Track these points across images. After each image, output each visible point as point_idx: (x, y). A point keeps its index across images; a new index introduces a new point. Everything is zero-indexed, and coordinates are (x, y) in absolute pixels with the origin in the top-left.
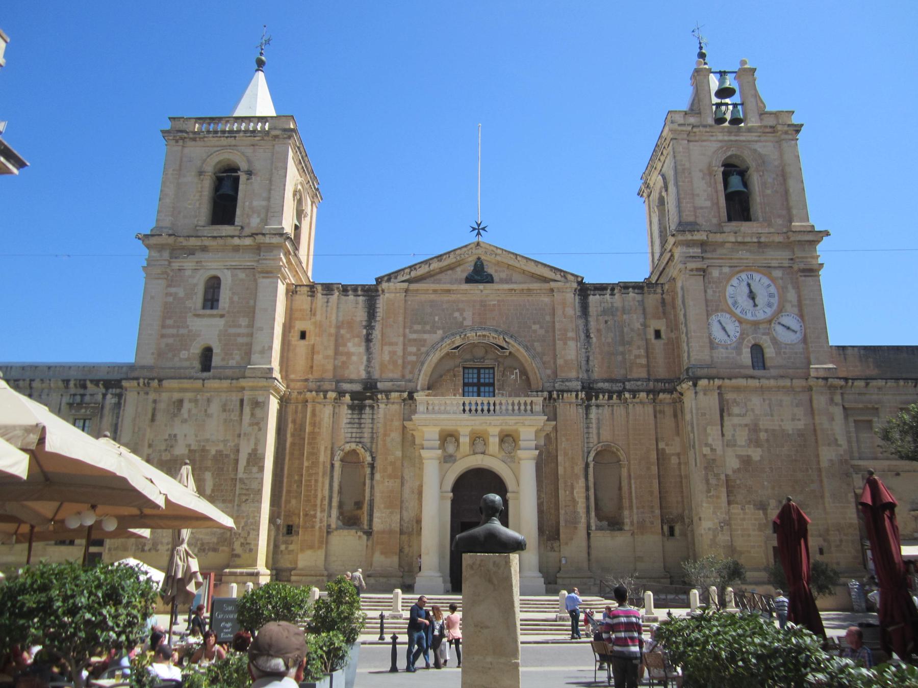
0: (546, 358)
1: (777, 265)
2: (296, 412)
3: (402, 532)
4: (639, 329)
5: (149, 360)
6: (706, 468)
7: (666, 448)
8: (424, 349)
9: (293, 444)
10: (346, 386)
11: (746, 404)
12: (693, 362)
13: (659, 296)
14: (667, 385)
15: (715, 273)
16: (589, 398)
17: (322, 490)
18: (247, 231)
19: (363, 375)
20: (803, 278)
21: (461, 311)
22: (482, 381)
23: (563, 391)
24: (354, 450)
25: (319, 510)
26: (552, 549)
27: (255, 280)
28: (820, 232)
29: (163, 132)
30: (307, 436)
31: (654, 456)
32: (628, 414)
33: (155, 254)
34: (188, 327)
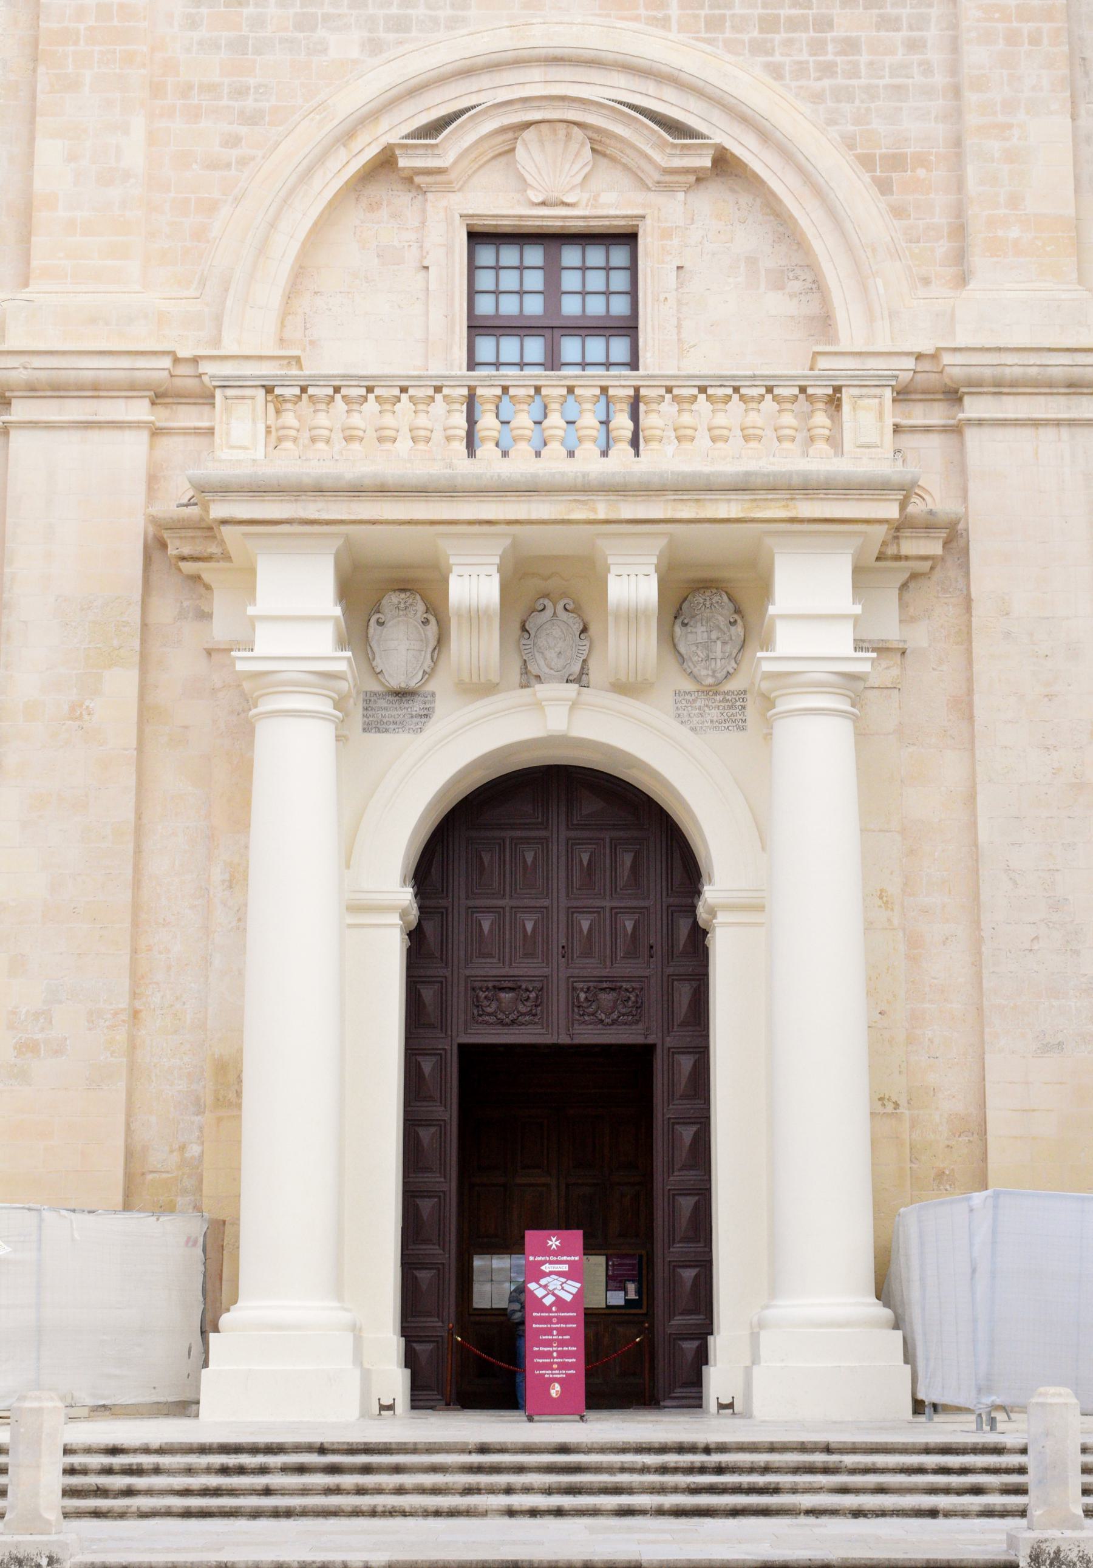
22: (571, 306)
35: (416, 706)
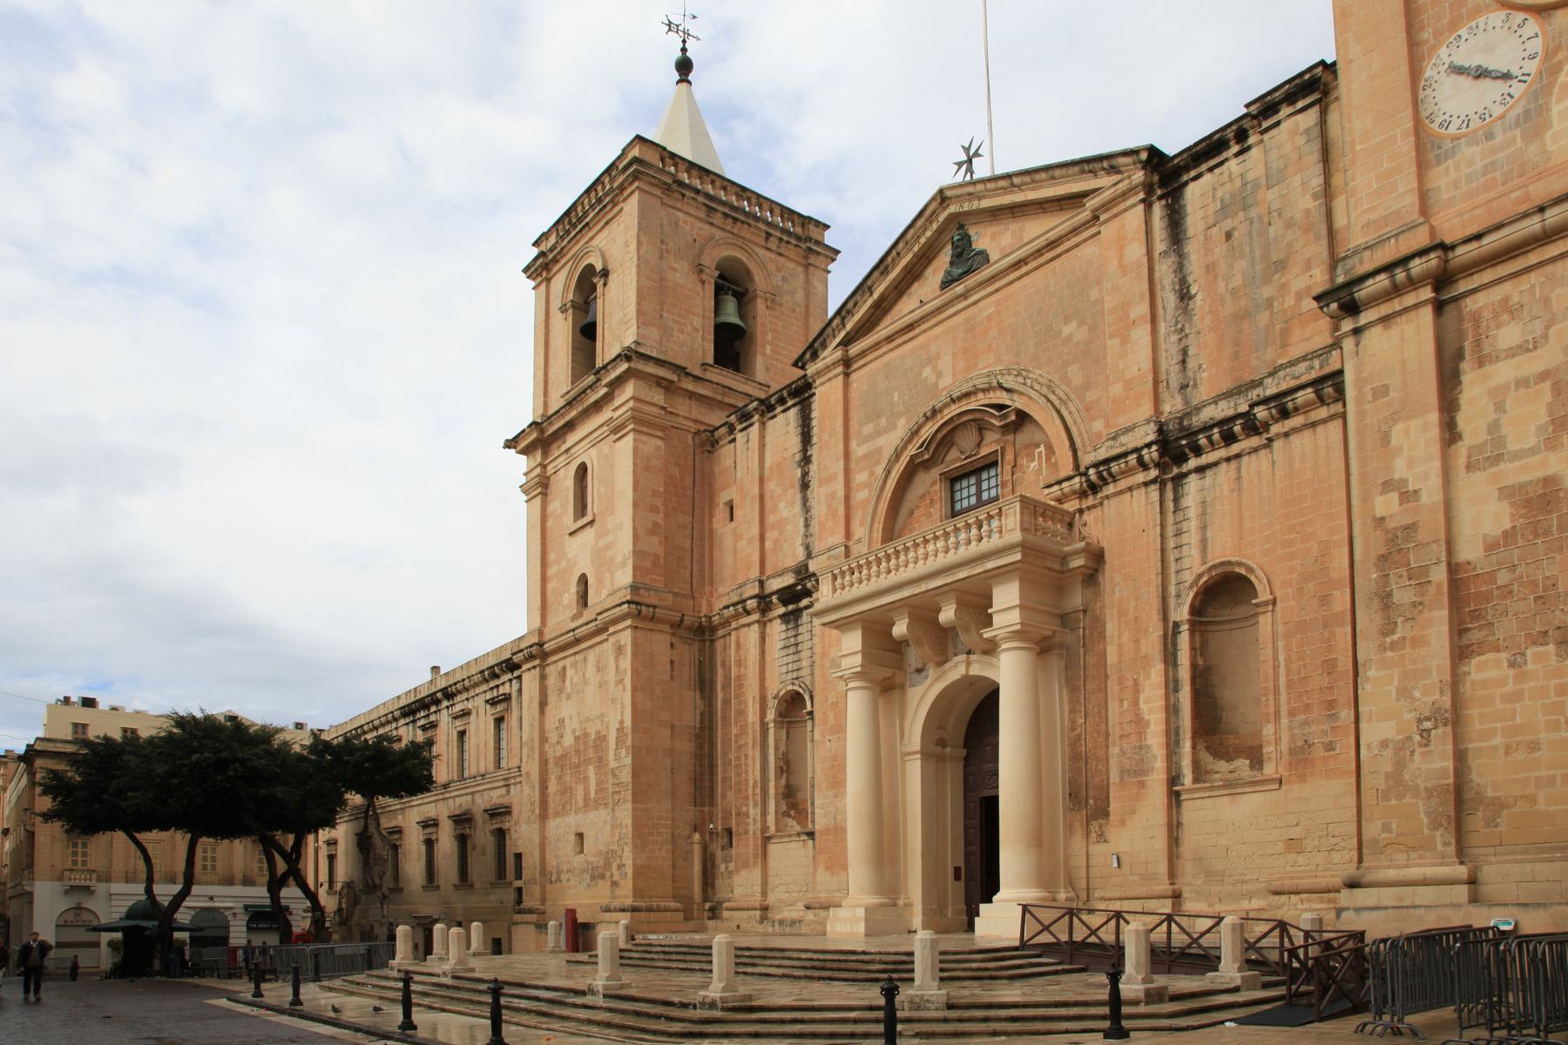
21: (932, 360)
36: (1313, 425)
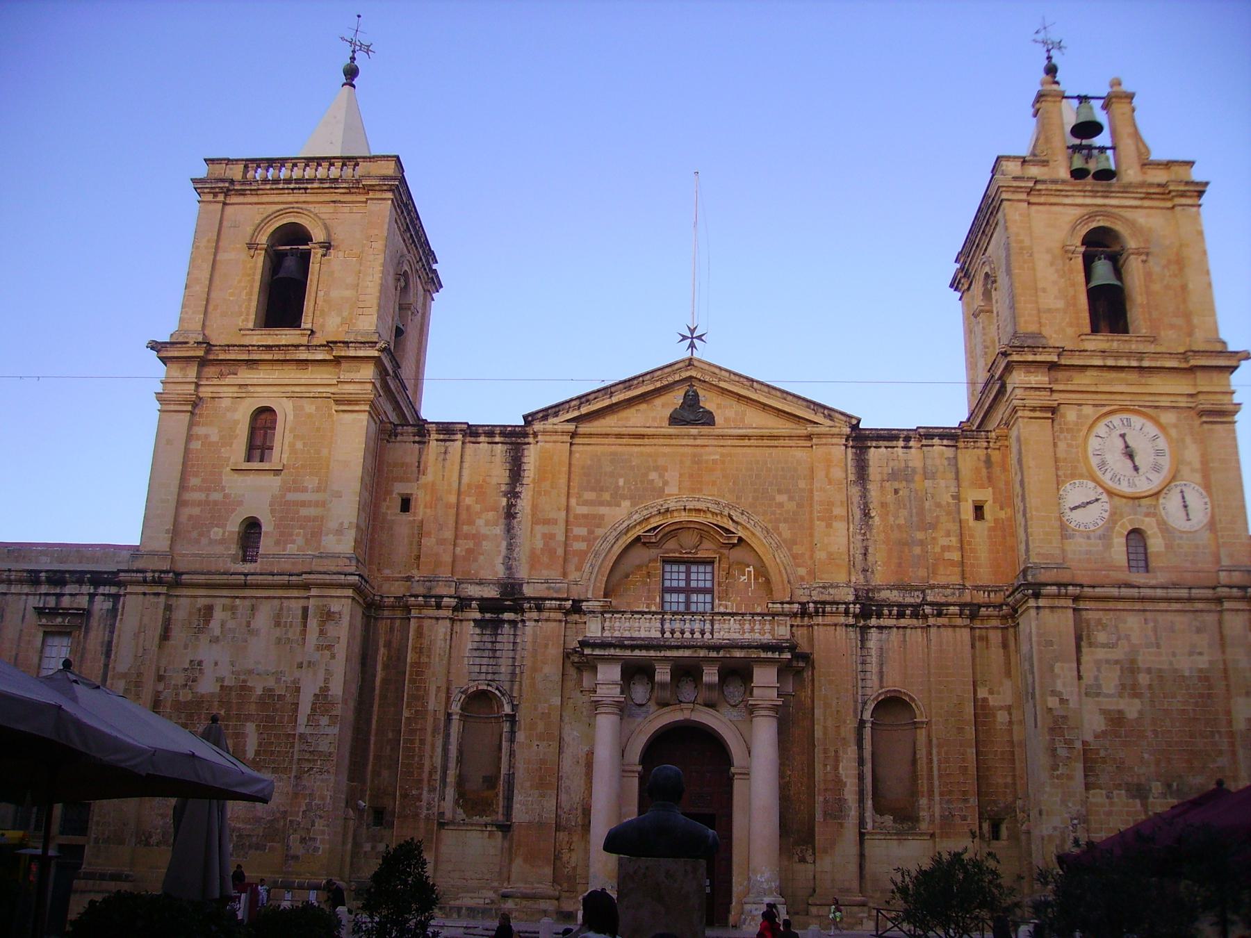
0: (797, 549)
1: (1169, 404)
2: (392, 629)
3: (558, 827)
4: (948, 503)
5: (162, 544)
6: (1052, 730)
7: (990, 698)
8: (599, 532)
9: (385, 681)
10: (473, 591)
11: (1116, 627)
12: (1034, 559)
13: (982, 453)
14: (992, 595)
15: (1070, 415)
16: (865, 614)
17: (431, 757)
18: (319, 339)
19: (501, 572)
20: (1209, 426)
21: (661, 470)
22: (693, 584)
23: (824, 603)
24: (484, 692)
25: (426, 789)
26: (803, 860)
27: (330, 415)
28: (1237, 353)
29: (194, 181)
30: (408, 668)
31: (969, 709)
32: (929, 640)
33: (176, 372)
34: (223, 489)
35: (644, 709)
36: (955, 627)
